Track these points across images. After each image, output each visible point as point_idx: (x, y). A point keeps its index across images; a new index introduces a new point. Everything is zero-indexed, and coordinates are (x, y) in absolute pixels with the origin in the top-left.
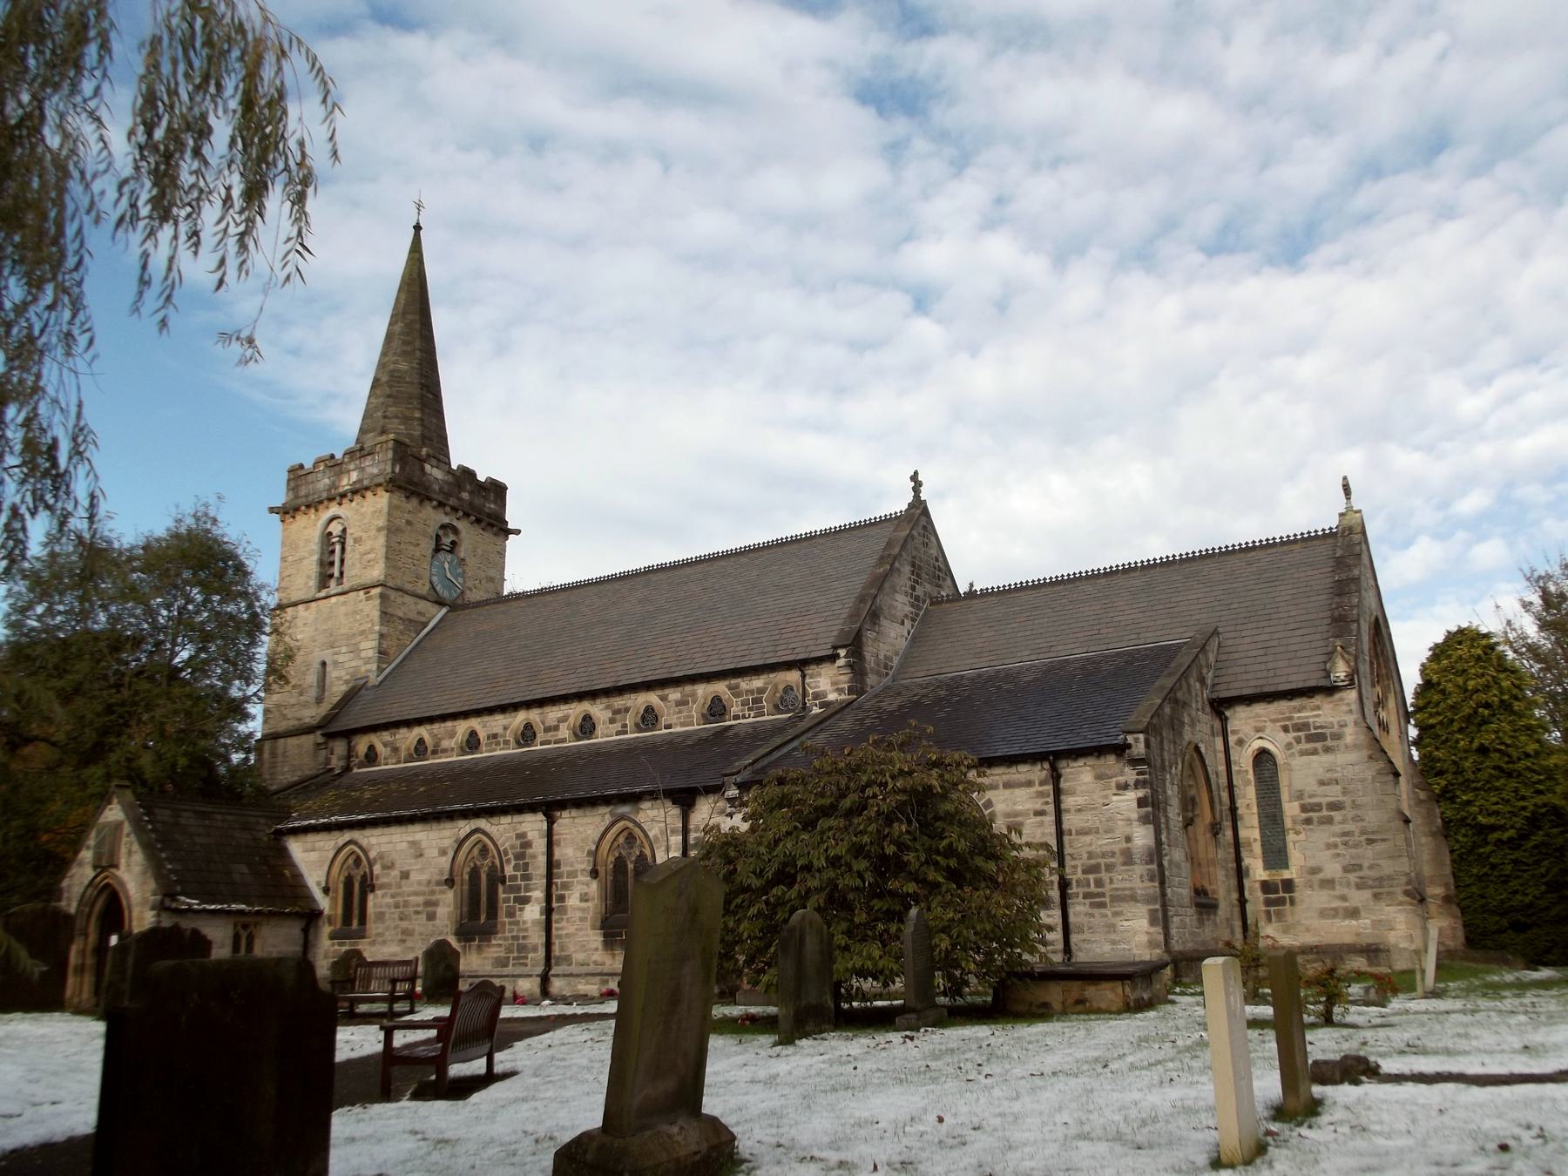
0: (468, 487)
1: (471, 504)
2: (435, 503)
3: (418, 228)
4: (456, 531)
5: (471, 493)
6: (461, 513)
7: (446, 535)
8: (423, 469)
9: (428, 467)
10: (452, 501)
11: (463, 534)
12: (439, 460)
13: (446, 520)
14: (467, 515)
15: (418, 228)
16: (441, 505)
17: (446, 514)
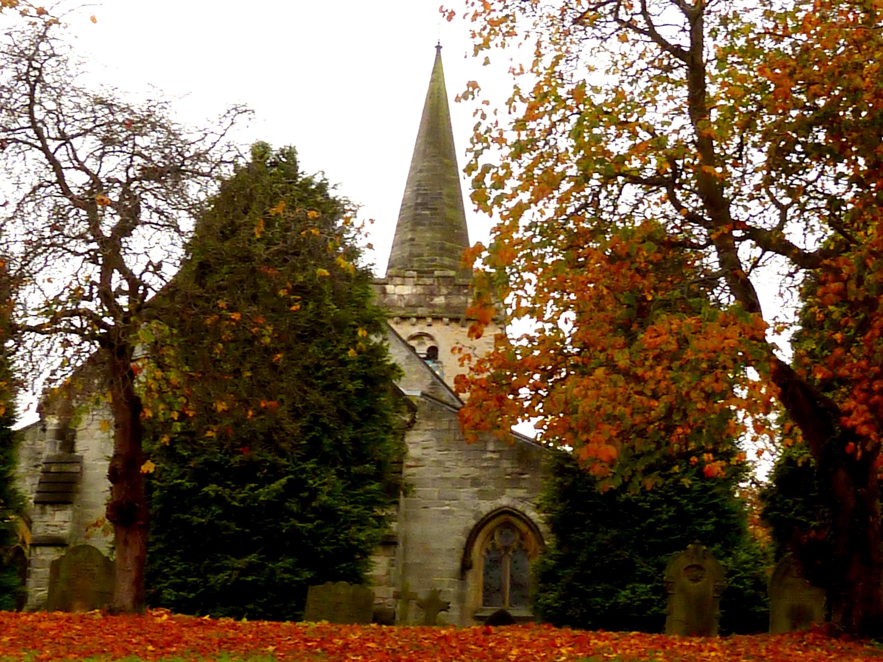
0: (444, 291)
1: (448, 306)
2: (396, 319)
3: (439, 48)
4: (432, 338)
5: (446, 296)
6: (429, 320)
7: (421, 344)
8: (384, 292)
9: (390, 288)
10: (420, 311)
11: (437, 338)
12: (404, 277)
13: (415, 330)
14: (437, 319)
15: (439, 48)
16: (404, 318)
17: (413, 325)
